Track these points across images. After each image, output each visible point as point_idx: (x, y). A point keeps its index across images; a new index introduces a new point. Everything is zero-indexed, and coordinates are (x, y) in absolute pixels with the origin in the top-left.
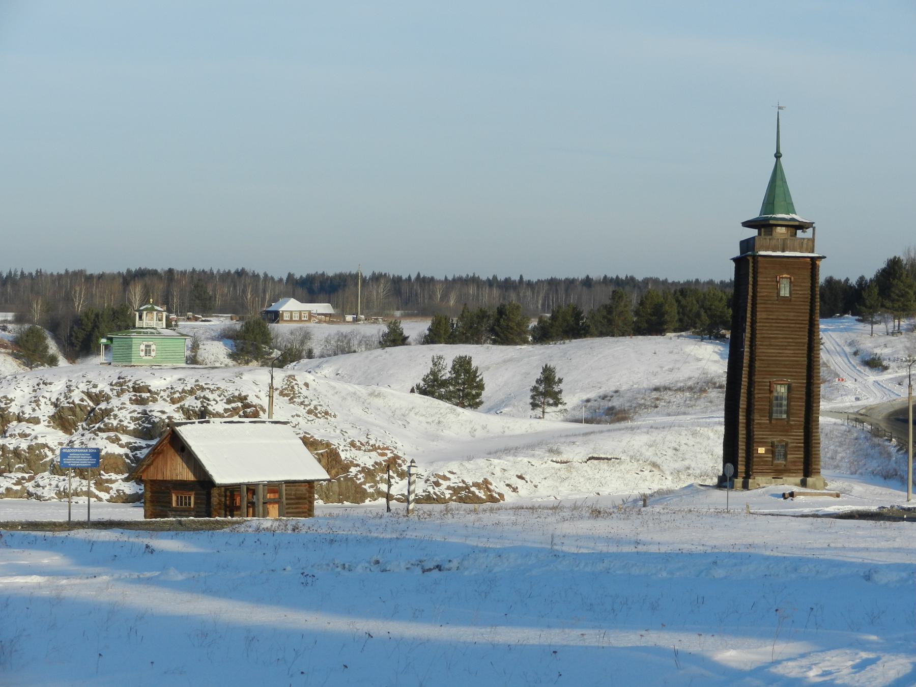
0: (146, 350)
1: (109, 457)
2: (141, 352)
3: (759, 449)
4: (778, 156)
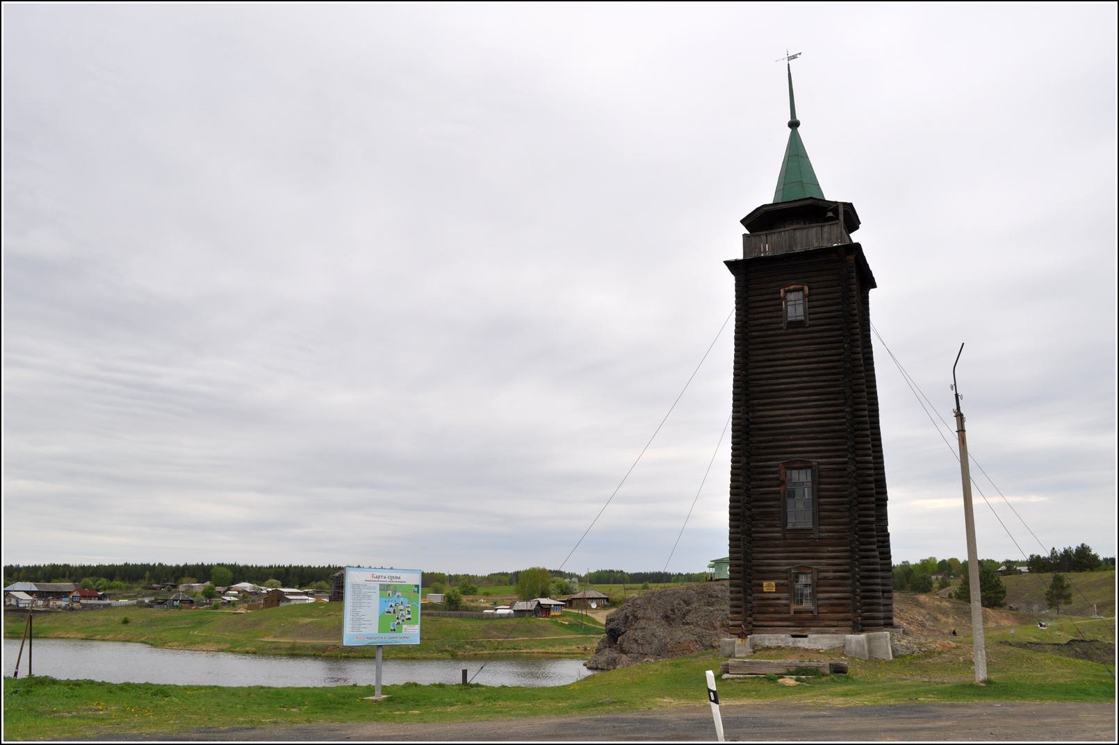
3: (765, 584)
4: (794, 124)
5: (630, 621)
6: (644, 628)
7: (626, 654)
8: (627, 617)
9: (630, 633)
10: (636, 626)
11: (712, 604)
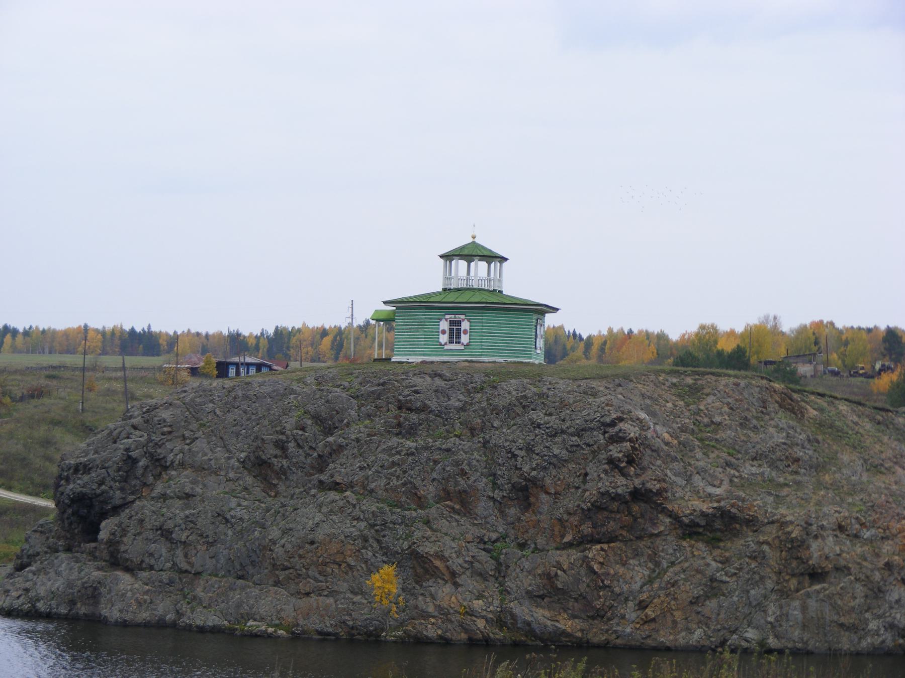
0: (451, 330)
1: (328, 539)
2: (441, 336)
5: (140, 472)
6: (188, 496)
7: (127, 570)
8: (131, 461)
9: (145, 507)
10: (159, 488)
11: (411, 432)
